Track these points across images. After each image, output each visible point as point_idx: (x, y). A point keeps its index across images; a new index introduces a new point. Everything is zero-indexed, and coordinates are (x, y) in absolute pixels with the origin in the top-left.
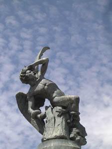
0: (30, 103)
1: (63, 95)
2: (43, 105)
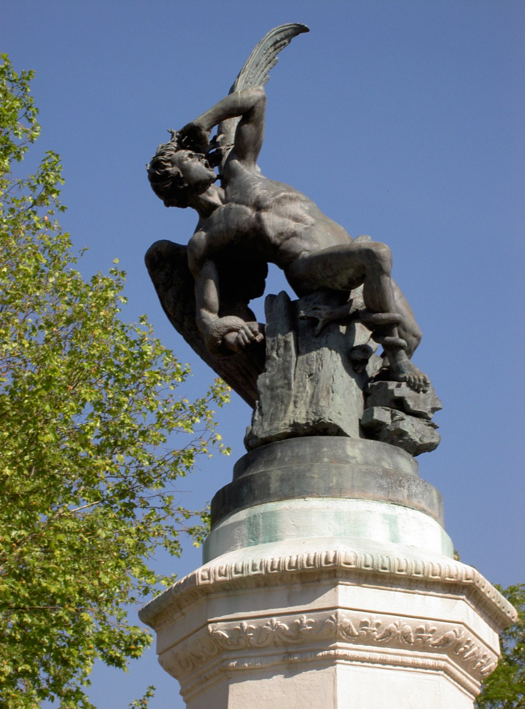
2: (260, 293)
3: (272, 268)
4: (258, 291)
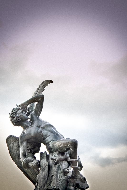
3: (43, 145)
4: (38, 151)
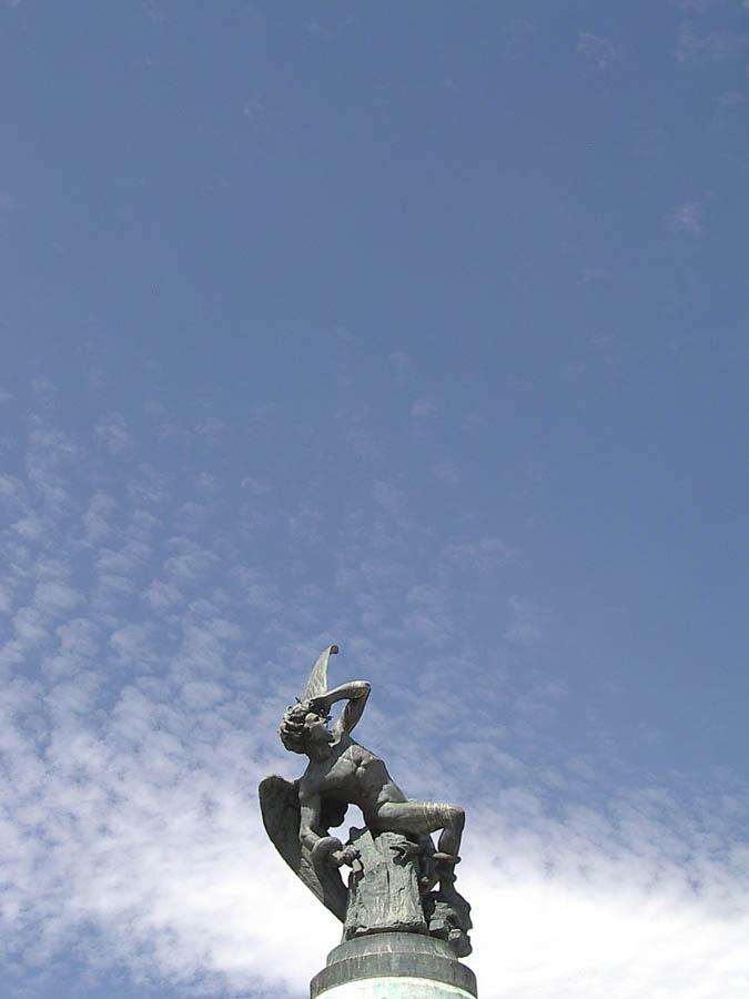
0: (308, 814)
1: (405, 801)
